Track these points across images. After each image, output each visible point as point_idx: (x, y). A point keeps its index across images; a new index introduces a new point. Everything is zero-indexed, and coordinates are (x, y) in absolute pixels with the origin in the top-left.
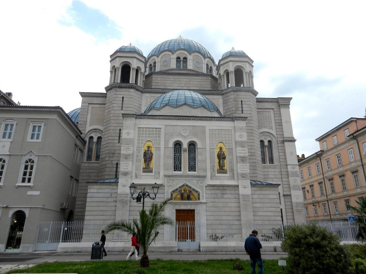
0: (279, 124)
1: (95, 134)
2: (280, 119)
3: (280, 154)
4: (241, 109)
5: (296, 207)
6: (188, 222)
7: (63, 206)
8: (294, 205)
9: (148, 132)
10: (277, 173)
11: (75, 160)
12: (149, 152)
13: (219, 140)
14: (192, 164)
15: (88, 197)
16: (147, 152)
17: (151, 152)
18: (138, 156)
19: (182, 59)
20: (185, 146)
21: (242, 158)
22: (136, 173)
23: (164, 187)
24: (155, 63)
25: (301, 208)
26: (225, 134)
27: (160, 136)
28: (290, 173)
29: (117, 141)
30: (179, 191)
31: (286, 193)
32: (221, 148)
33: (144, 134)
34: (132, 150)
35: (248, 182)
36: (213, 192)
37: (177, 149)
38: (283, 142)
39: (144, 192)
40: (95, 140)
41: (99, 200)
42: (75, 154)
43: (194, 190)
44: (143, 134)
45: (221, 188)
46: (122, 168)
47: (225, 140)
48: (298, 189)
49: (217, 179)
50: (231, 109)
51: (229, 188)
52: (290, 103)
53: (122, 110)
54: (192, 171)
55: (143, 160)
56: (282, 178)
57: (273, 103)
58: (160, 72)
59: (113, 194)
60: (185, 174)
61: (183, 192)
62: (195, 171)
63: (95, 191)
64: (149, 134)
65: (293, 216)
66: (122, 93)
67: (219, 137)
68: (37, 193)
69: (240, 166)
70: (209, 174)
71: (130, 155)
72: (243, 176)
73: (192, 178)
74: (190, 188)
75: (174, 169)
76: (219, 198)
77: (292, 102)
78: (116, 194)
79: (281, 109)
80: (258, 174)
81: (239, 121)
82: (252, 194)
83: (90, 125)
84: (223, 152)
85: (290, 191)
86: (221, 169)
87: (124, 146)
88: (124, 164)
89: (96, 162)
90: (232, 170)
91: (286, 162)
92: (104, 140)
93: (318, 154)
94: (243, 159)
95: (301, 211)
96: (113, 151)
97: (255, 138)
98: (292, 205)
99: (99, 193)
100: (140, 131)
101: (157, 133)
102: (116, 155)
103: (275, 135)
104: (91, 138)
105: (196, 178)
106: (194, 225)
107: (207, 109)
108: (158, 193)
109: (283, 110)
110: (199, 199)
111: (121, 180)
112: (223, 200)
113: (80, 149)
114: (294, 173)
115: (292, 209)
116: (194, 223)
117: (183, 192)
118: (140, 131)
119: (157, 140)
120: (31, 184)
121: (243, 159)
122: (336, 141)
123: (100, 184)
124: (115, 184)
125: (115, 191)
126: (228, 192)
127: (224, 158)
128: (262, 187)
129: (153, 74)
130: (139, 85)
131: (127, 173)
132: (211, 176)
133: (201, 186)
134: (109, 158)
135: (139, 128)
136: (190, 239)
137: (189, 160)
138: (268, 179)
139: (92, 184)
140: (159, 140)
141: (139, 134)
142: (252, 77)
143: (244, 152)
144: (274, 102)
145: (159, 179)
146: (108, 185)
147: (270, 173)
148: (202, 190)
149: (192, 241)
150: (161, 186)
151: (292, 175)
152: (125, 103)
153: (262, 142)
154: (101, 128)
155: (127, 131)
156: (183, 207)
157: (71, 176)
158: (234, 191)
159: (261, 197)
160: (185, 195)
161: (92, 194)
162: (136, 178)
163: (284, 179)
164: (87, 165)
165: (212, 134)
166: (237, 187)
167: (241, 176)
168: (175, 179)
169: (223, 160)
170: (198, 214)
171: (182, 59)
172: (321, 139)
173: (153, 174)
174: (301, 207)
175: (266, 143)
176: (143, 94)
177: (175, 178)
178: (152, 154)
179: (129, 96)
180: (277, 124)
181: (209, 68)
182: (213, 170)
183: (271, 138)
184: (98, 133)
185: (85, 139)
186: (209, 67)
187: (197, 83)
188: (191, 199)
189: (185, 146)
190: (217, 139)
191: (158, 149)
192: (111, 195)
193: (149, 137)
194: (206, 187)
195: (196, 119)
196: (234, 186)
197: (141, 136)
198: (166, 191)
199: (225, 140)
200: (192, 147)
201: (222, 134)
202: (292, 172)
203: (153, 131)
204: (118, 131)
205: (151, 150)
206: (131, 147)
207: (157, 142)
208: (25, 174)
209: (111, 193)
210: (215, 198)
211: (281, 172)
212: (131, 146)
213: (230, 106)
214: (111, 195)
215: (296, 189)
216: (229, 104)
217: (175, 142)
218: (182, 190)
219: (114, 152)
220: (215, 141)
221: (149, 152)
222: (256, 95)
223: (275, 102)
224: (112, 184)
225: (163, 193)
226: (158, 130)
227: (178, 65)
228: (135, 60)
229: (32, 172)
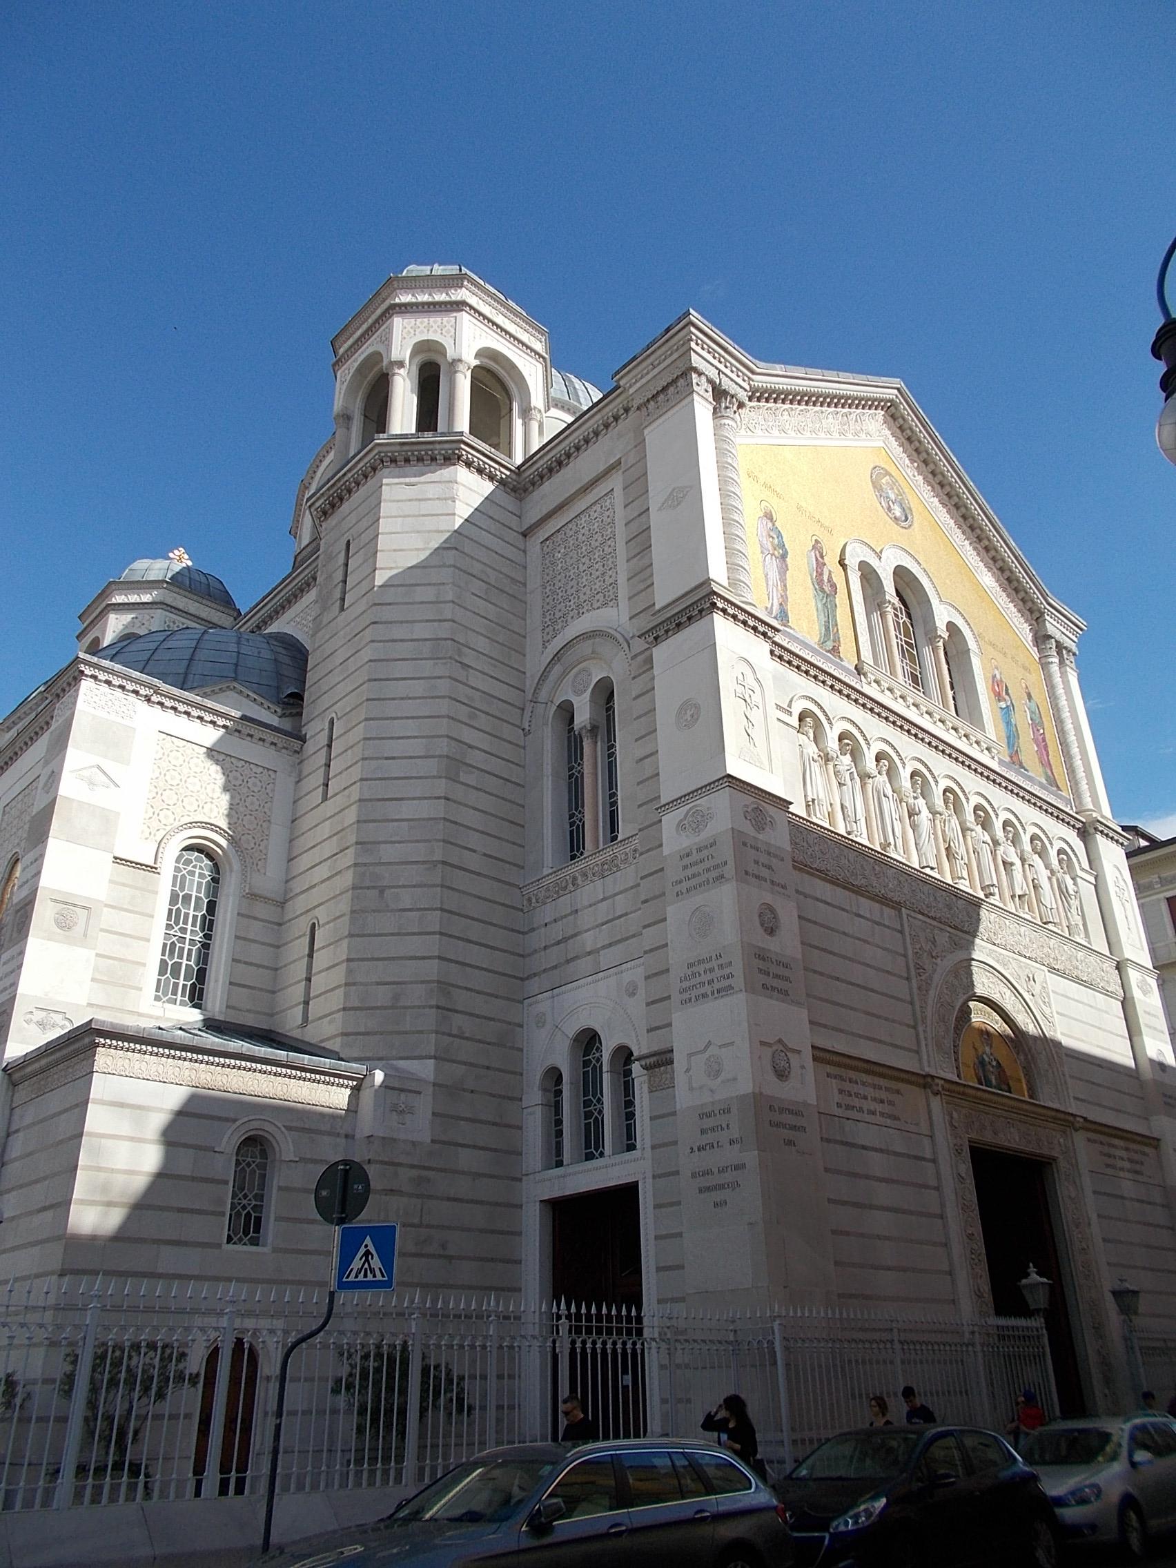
10: (621, 904)
25: (737, 1147)
48: (717, 986)
95: (734, 1185)
174: (732, 1142)
175: (583, 717)
215: (707, 989)
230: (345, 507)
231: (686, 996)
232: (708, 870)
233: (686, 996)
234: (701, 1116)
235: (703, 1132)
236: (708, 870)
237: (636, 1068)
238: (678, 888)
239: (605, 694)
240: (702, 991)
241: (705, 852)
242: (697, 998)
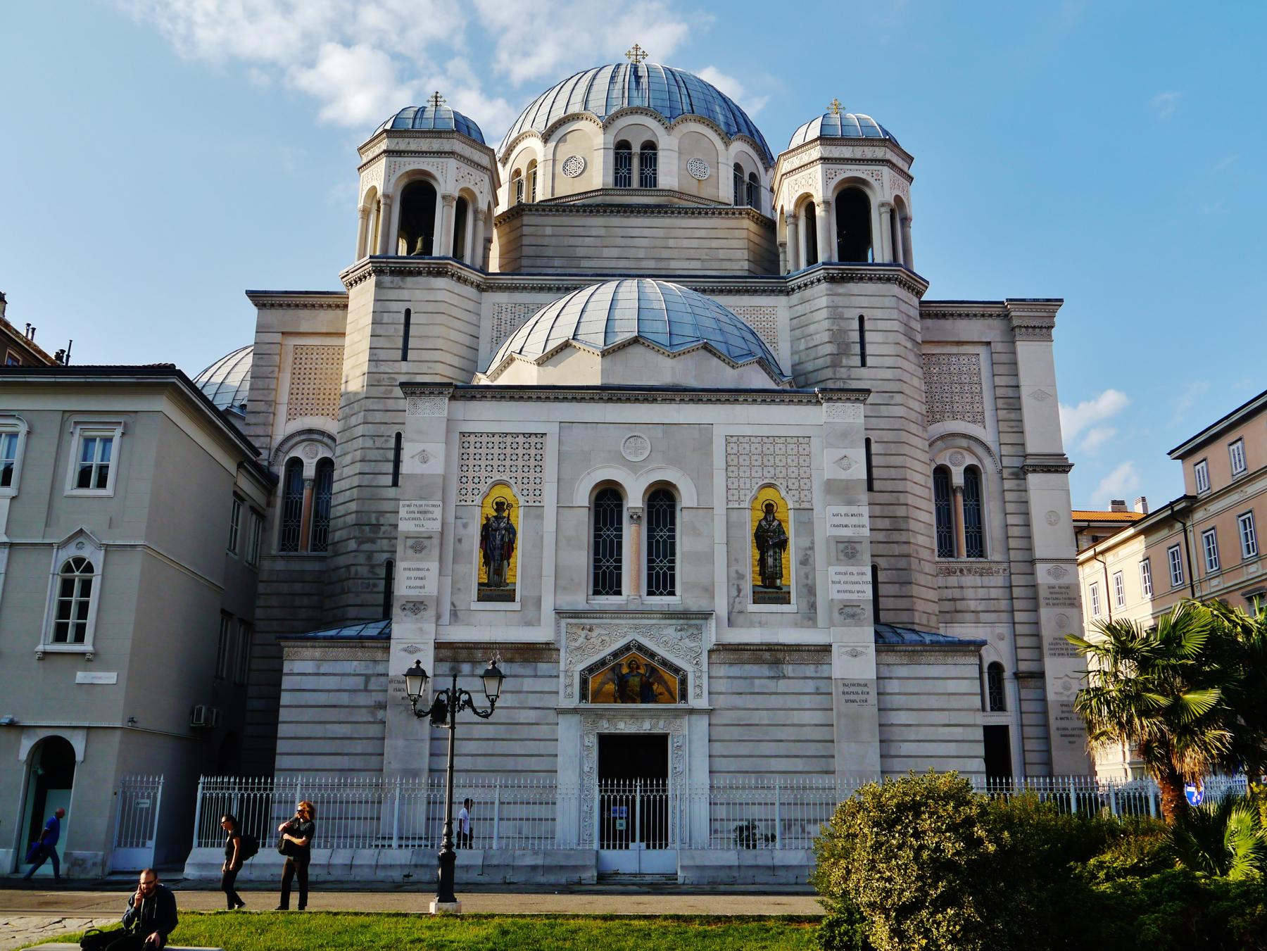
0: (1012, 403)
1: (307, 449)
2: (1014, 384)
3: (1011, 520)
4: (857, 349)
5: (1061, 719)
6: (636, 782)
7: (199, 718)
8: (1053, 713)
9: (496, 451)
10: (994, 593)
11: (237, 551)
12: (502, 525)
13: (764, 477)
14: (661, 569)
15: (286, 690)
16: (495, 525)
17: (508, 523)
18: (460, 541)
19: (636, 149)
20: (635, 499)
21: (846, 544)
22: (453, 604)
23: (554, 654)
24: (533, 164)
26: (786, 455)
27: (540, 463)
28: (1043, 593)
29: (388, 480)
30: (613, 669)
31: (1023, 667)
32: (769, 508)
33: (483, 458)
34: (439, 517)
35: (867, 633)
36: (735, 671)
37: (605, 511)
38: (1021, 473)
39: (454, 691)
40: (309, 471)
41: (322, 698)
42: (236, 530)
43: (665, 663)
44: (477, 457)
45: (767, 655)
46: (404, 586)
47: (787, 478)
48: (1070, 652)
49: (752, 625)
50: (820, 347)
51: (796, 656)
52: (1057, 319)
53: (405, 358)
54: (661, 594)
55: (477, 555)
56: (1012, 611)
57: (990, 322)
58: (553, 203)
59: (373, 679)
60: (632, 607)
61: (625, 671)
62: (672, 593)
63: (309, 667)
64: (502, 457)
65: (1049, 751)
66: (404, 294)
67: (763, 466)
68: (109, 678)
69: (839, 573)
70: (721, 606)
71: (430, 538)
72: (848, 612)
73: (660, 619)
74: (652, 655)
75: (596, 584)
76: (758, 693)
77: (1060, 317)
78: (382, 679)
79: (1018, 343)
80: (914, 599)
81: (839, 404)
82: (878, 678)
83: (291, 416)
84: (776, 523)
85: (1040, 659)
86: (764, 586)
87: (408, 502)
88: (409, 569)
89: (315, 553)
90: (811, 590)
91: (1030, 549)
92: (342, 474)
93: (1176, 509)
94: (848, 550)
96: (373, 516)
97: (909, 462)
98: (1045, 712)
99: (323, 674)
100: (466, 445)
101: (533, 452)
102: (384, 533)
103: (994, 447)
104: (296, 464)
105: (674, 621)
106: (664, 791)
107: (719, 358)
108: (503, 692)
109: (1026, 349)
110: (684, 696)
111: (403, 629)
112: (774, 701)
113: (254, 510)
114: (1059, 590)
115: (1046, 725)
116: (664, 784)
117: (625, 671)
118: (466, 445)
119: (532, 479)
120: (87, 646)
121: (848, 550)
122: (1240, 461)
123: (324, 644)
124: (379, 645)
125: (380, 669)
126: (789, 670)
127: (783, 544)
128: (918, 651)
129: (523, 210)
130: (468, 260)
131: (422, 602)
132: (729, 614)
133: (691, 649)
134: (360, 543)
135: (463, 434)
136: (642, 840)
137: (650, 553)
138: (960, 615)
139: (297, 644)
140: (538, 481)
141: (465, 457)
142: (906, 220)
143: (854, 521)
144: (991, 315)
145: (540, 625)
146: (355, 647)
147: (969, 593)
148: (697, 664)
149: (648, 847)
150: (545, 649)
151: (1051, 601)
152: (417, 334)
153: (942, 474)
154: (331, 426)
155: (421, 447)
156: (624, 727)
157: (223, 611)
158: (812, 667)
159: (913, 686)
160: (635, 681)
161: (299, 678)
162: (456, 622)
163: (1019, 616)
164: (280, 565)
165: (738, 455)
166: (826, 651)
167: (840, 614)
168: (599, 626)
169: (775, 553)
170: (680, 753)
171: (636, 149)
172: (1187, 452)
173: (515, 606)
175: (958, 479)
176: (485, 294)
177: (596, 621)
178: (511, 531)
179: (430, 307)
180: (1000, 403)
181: (743, 182)
182: (739, 590)
183: (977, 457)
184: (319, 445)
185: (275, 469)
186: (746, 178)
187: (695, 243)
189: (635, 499)
190: (754, 474)
191: (535, 511)
192: (367, 683)
193: (501, 469)
194: (710, 652)
195: (678, 399)
196: (814, 651)
197: (471, 467)
198: (562, 666)
199: (787, 478)
200: (664, 504)
201: (774, 454)
202: (1049, 588)
203: (515, 446)
204: (392, 443)
205: (508, 519)
206: (433, 506)
207: (531, 487)
208: (64, 609)
209: (367, 677)
210: (741, 694)
211: (1011, 587)
212: (431, 503)
213: (818, 336)
214: (367, 683)
215: (1064, 652)
216: (812, 328)
217: (597, 485)
218: (620, 665)
219: (378, 520)
220: (748, 481)
221: (502, 525)
222: (919, 294)
223: (999, 316)
224: (370, 644)
225: (551, 676)
226: (533, 440)
227: (623, 172)
228: (452, 163)
229: (87, 603)
230: (852, 287)
231: (1053, 652)
232: (1065, 599)
233: (1053, 652)
234: (1062, 705)
235: (1063, 712)
236: (1065, 599)
237: (1007, 674)
238: (1048, 601)
239: (972, 473)
240: (1062, 652)
241: (1063, 590)
242: (1059, 654)
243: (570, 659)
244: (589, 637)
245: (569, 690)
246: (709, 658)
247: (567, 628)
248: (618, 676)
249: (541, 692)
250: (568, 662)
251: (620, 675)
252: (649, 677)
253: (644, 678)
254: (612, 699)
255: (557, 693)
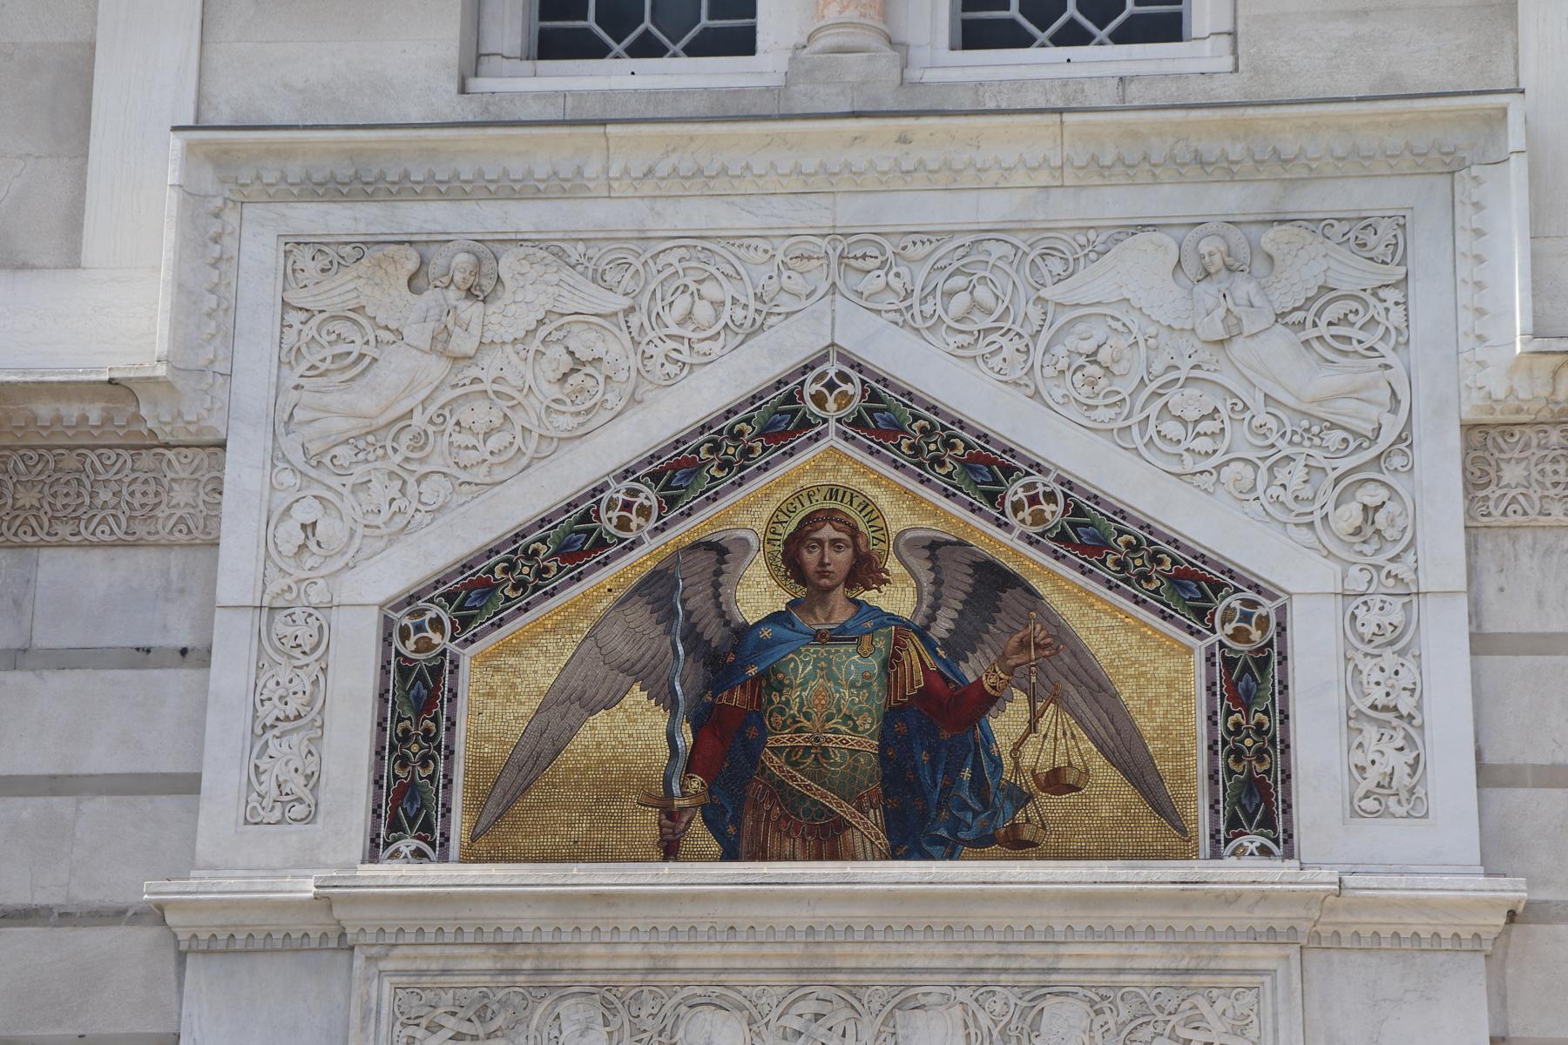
145: (72, 260)
188: (1021, 798)
225: (143, 655)
243: (305, 512)
244: (463, 343)
245: (286, 754)
246: (1477, 480)
247: (291, 274)
248: (692, 636)
249: (54, 785)
250: (290, 535)
251: (714, 633)
252: (960, 645)
253: (913, 653)
254: (648, 823)
255: (188, 785)
